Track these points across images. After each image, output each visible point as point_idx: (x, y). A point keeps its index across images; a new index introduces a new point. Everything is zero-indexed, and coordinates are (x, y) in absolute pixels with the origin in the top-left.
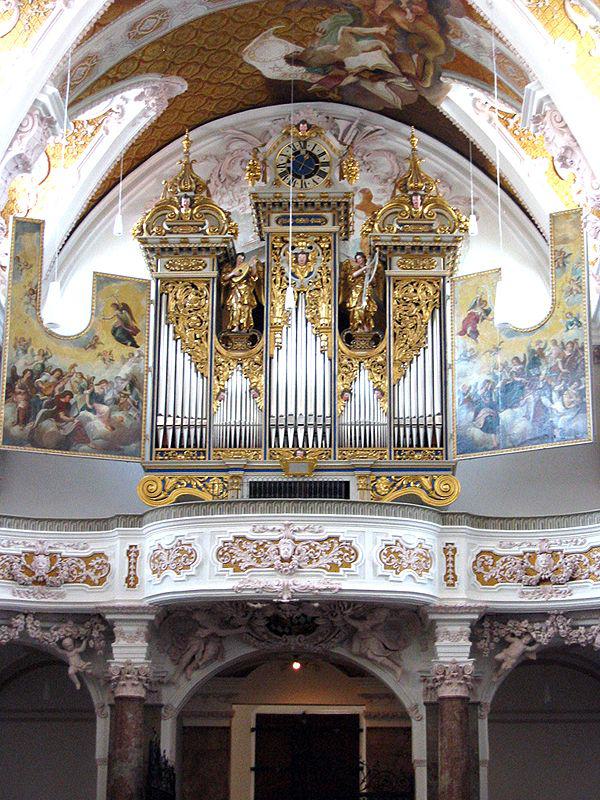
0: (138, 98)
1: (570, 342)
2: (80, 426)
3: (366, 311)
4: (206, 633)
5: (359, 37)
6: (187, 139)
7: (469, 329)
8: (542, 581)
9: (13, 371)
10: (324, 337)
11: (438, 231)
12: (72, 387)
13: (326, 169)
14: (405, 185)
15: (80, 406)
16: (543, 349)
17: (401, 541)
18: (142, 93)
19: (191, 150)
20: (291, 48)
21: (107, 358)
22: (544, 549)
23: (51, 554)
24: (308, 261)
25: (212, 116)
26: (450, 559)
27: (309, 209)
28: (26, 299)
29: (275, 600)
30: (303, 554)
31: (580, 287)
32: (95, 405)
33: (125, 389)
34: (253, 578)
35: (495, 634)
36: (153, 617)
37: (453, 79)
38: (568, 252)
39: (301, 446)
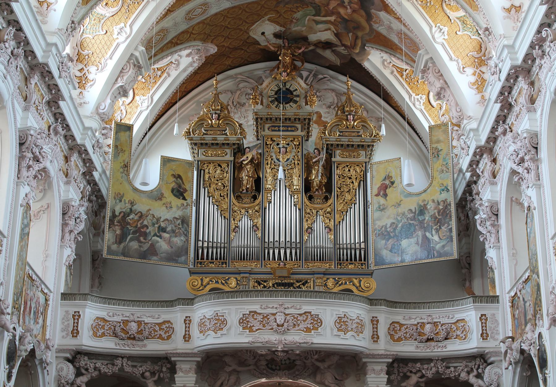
0: (188, 55)
1: (443, 201)
2: (152, 245)
3: (320, 182)
4: (230, 369)
5: (317, 23)
6: (216, 80)
7: (381, 193)
8: (428, 340)
9: (113, 212)
10: (295, 197)
11: (363, 136)
12: (148, 222)
13: (298, 99)
14: (344, 109)
15: (152, 234)
17: (347, 315)
18: (191, 53)
19: (218, 86)
20: (278, 28)
21: (169, 206)
22: (430, 321)
23: (138, 321)
24: (286, 152)
25: (229, 68)
26: (375, 326)
27: (288, 122)
28: (121, 170)
29: (274, 349)
30: (290, 321)
31: (448, 169)
32: (161, 233)
33: (179, 224)
34: (261, 336)
35: (401, 371)
36: (199, 359)
37: (373, 48)
38: (440, 148)
39: (282, 260)
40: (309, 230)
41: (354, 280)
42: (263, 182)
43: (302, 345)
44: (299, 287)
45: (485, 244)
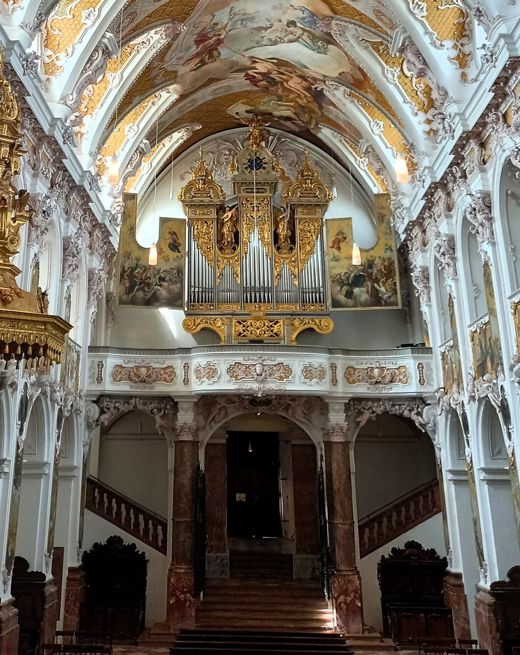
16: (375, 260)
24: (258, 210)
27: (259, 185)
40: (279, 277)
41: (316, 320)
42: (241, 235)
43: (277, 392)
44: (271, 326)
45: (419, 298)
